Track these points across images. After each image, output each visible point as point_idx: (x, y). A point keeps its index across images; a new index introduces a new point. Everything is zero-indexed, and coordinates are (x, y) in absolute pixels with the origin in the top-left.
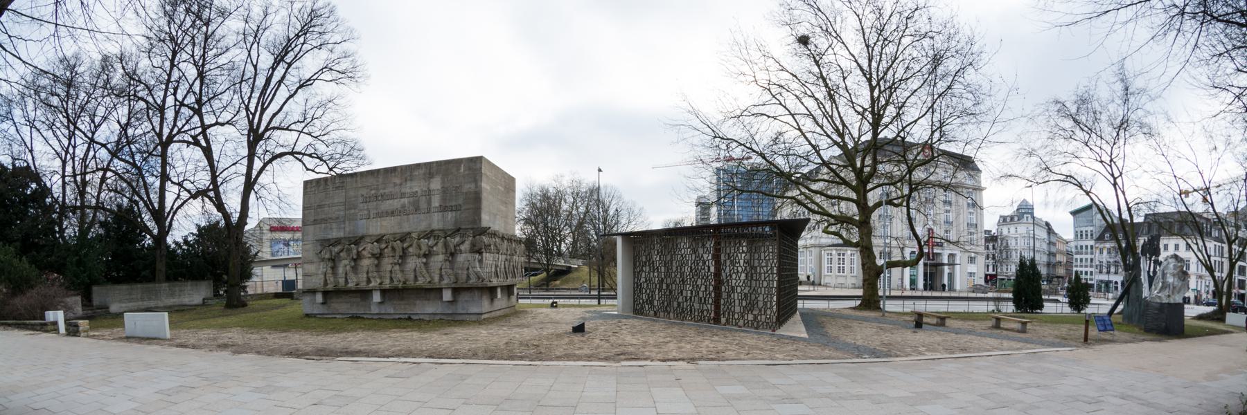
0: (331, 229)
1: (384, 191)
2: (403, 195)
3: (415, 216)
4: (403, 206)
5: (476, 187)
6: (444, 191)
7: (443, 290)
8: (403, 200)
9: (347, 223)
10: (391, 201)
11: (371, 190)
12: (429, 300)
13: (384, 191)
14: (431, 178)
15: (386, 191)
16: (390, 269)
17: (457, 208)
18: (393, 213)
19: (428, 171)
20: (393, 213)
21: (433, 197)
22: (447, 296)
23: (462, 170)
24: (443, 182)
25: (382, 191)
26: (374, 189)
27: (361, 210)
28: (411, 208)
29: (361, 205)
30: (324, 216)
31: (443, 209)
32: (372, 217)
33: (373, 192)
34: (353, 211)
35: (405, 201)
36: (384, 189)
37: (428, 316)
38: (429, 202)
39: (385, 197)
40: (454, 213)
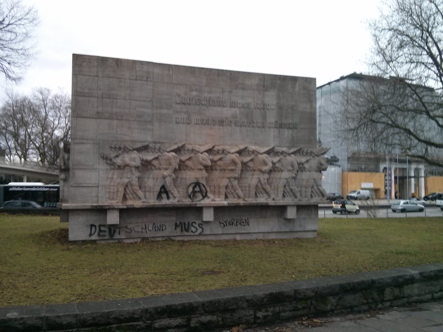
0: (130, 128)
1: (210, 95)
2: (233, 105)
3: (249, 128)
4: (234, 116)
5: (311, 108)
6: (280, 108)
7: (288, 208)
8: (233, 110)
9: (156, 124)
10: (219, 109)
11: (192, 90)
12: (265, 218)
13: (210, 95)
14: (266, 91)
15: (212, 95)
16: (226, 184)
17: (293, 127)
18: (221, 122)
19: (262, 83)
20: (221, 122)
21: (267, 111)
22: (291, 213)
23: (297, 89)
24: (278, 98)
25: (206, 95)
26: (196, 90)
27: (177, 112)
28: (244, 120)
29: (178, 106)
30: (115, 110)
31: (280, 126)
32: (193, 123)
33: (194, 93)
34: (165, 111)
35: (236, 111)
36: (210, 92)
37: (262, 235)
38: (264, 117)
39: (210, 103)
40: (290, 131)
